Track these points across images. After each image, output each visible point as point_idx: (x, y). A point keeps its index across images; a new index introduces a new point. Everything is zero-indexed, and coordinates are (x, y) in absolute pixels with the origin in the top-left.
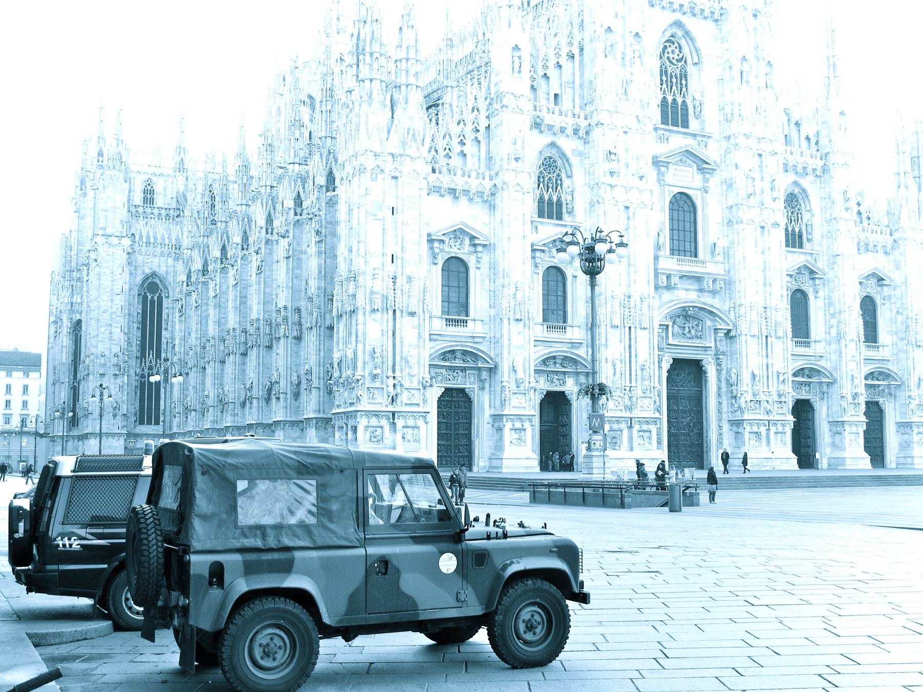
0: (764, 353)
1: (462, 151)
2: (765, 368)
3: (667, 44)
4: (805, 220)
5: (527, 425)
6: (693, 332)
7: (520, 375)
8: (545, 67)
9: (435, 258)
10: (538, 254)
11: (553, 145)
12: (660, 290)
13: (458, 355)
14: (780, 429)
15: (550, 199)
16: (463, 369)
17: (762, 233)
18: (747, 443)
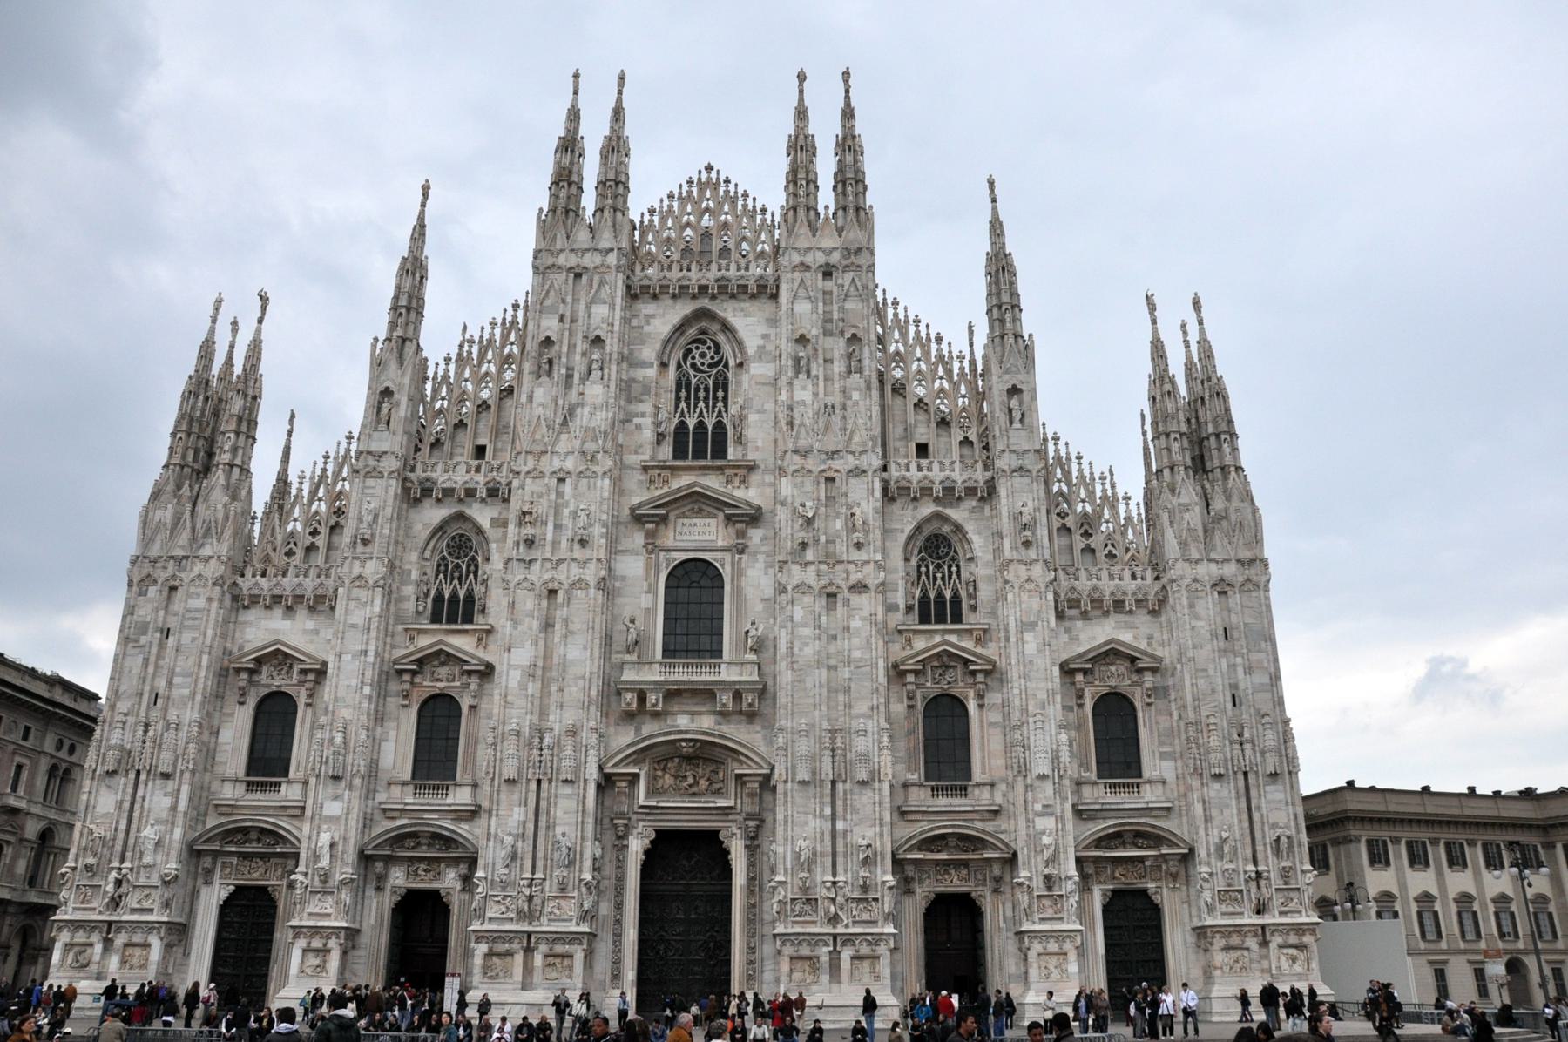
0: (828, 811)
1: (313, 544)
2: (827, 838)
3: (693, 347)
4: (965, 574)
5: (332, 943)
6: (703, 783)
7: (325, 862)
9: (242, 695)
10: (407, 677)
11: (460, 517)
12: (638, 719)
13: (253, 835)
14: (865, 950)
15: (454, 595)
16: (262, 856)
18: (784, 978)
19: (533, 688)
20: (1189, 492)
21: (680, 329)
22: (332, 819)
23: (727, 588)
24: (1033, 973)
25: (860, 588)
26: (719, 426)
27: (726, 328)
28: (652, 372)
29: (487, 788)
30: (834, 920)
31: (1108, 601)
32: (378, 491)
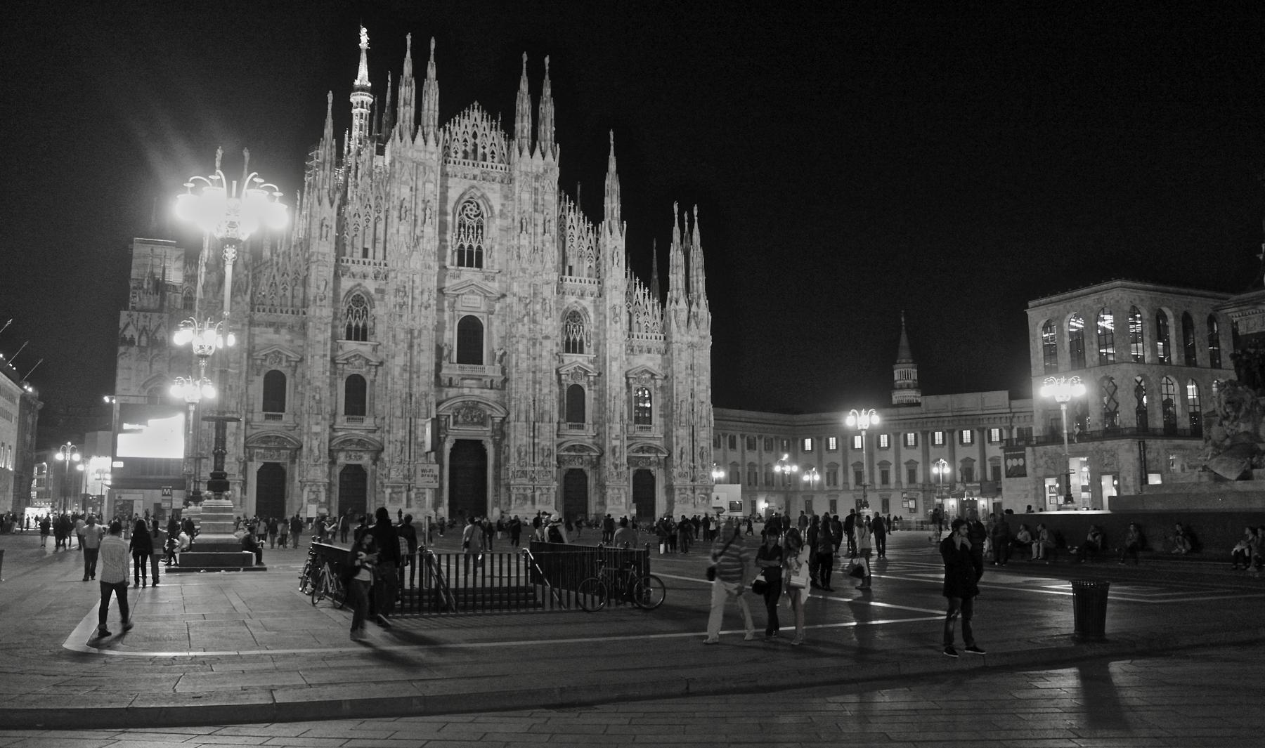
8: (356, 230)
11: (359, 285)
15: (357, 326)
17: (534, 345)
19: (406, 376)
20: (683, 304)
21: (464, 194)
22: (316, 434)
23: (485, 330)
24: (608, 501)
25: (547, 337)
26: (479, 248)
27: (483, 196)
28: (450, 218)
29: (387, 421)
30: (533, 479)
31: (645, 349)
32: (325, 274)
